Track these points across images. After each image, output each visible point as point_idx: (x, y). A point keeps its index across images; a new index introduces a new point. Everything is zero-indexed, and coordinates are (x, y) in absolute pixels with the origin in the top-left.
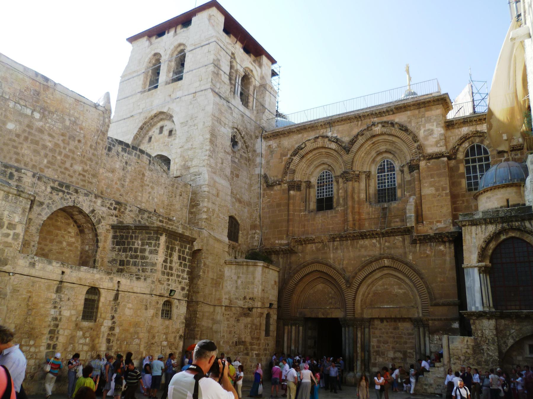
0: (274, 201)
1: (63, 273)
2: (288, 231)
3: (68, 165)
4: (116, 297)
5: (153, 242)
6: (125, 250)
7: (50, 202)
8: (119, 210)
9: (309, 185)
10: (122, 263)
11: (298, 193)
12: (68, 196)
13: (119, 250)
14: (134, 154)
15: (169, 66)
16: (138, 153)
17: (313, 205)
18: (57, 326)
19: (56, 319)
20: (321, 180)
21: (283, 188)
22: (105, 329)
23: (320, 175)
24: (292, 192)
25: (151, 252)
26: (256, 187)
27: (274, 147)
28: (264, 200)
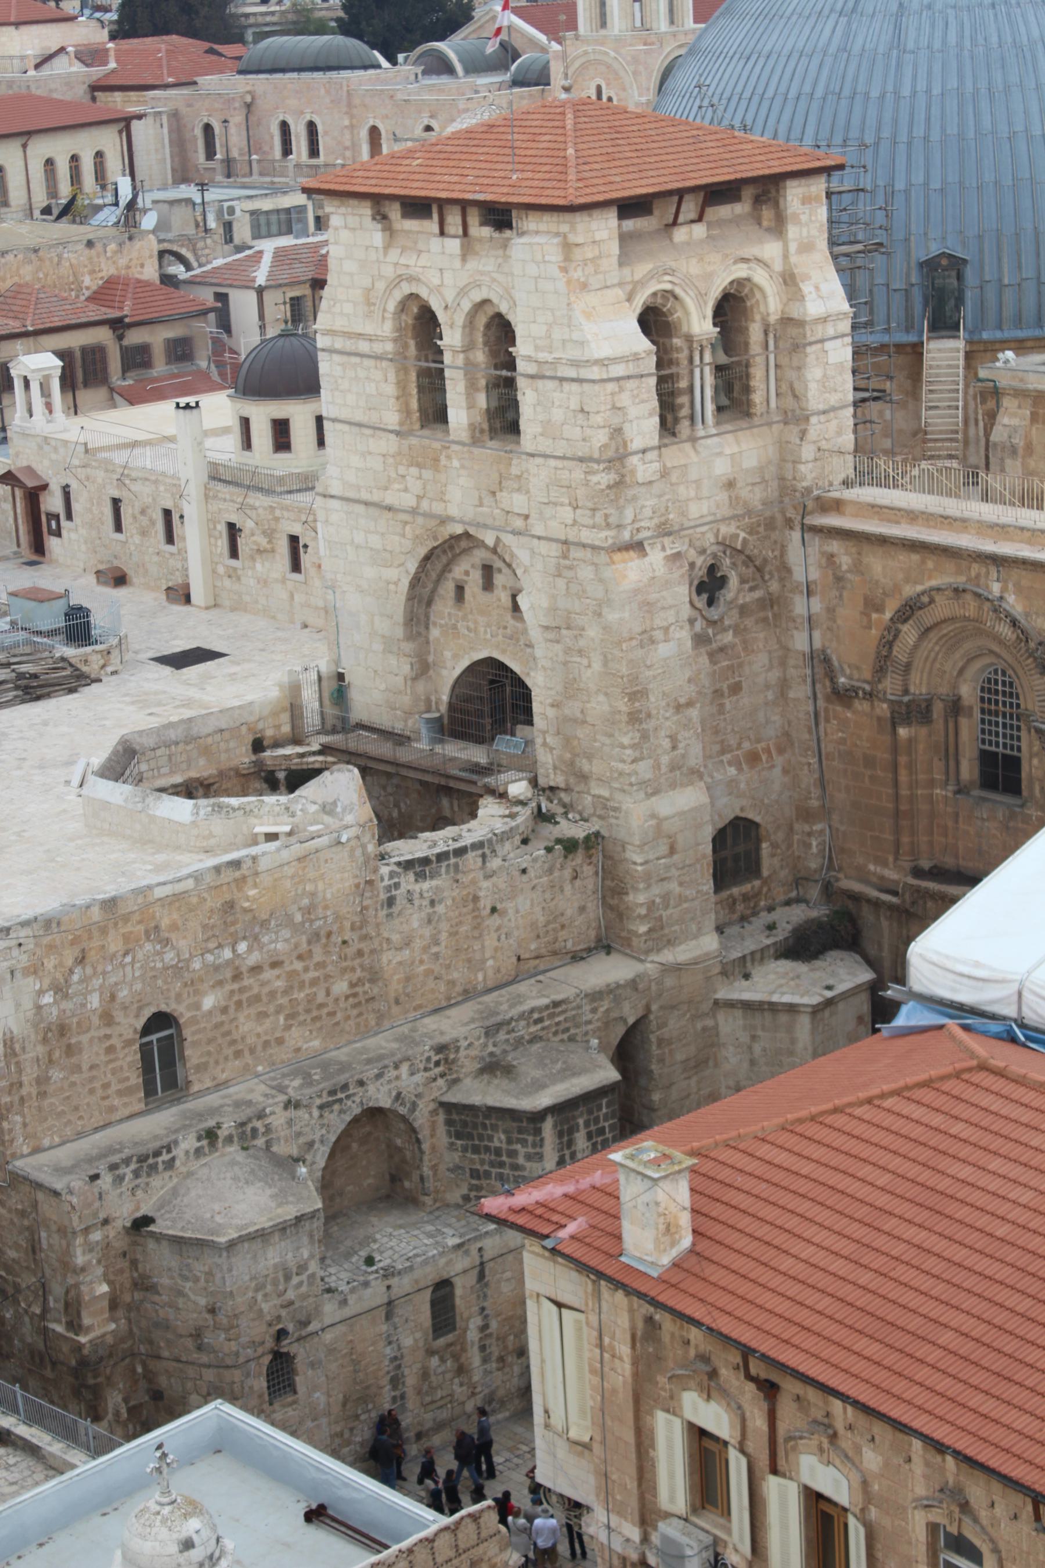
0: (856, 745)
1: (389, 1287)
2: (897, 844)
3: (321, 998)
4: (481, 1276)
5: (530, 1139)
6: (476, 1150)
7: (324, 1131)
8: (446, 1060)
9: (955, 708)
10: (475, 1174)
11: (923, 731)
12: (349, 1103)
14: (443, 870)
15: (469, 366)
16: (453, 861)
17: (968, 769)
18: (399, 1367)
19: (395, 1358)
20: (989, 691)
21: (878, 711)
22: (473, 1335)
23: (985, 675)
24: (903, 732)
25: (529, 1157)
26: (800, 692)
27: (845, 567)
28: (829, 730)
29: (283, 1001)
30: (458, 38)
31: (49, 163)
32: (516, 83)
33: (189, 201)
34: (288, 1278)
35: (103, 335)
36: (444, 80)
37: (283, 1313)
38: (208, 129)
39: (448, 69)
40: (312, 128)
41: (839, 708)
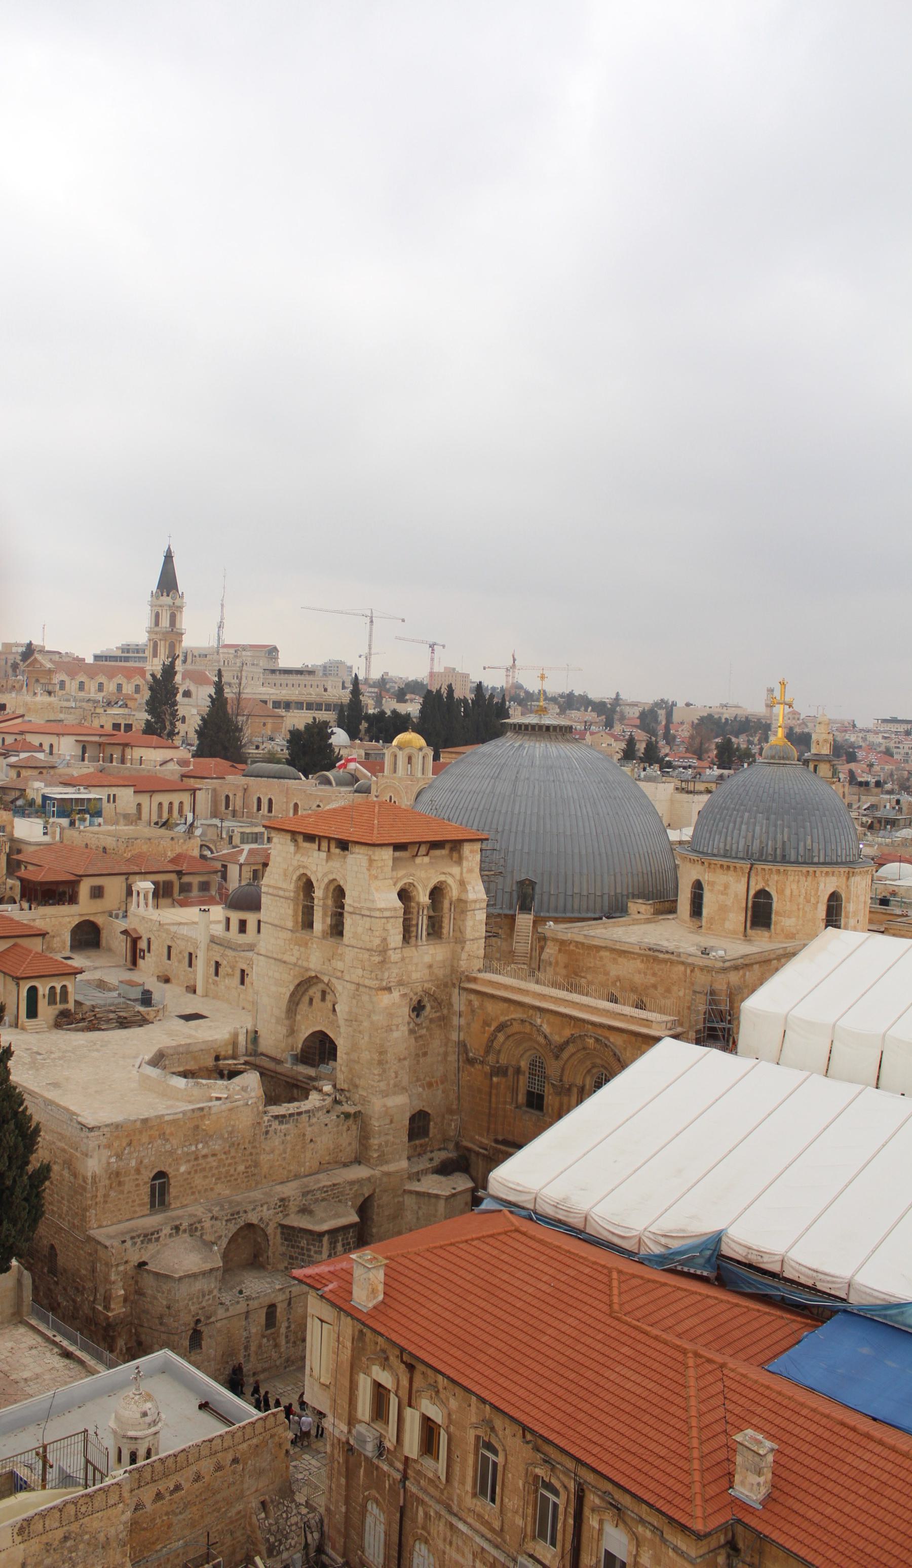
2: (489, 1129)
3: (232, 1172)
4: (289, 1304)
6: (293, 1247)
9: (518, 1071)
10: (291, 1257)
11: (504, 1080)
13: (288, 1246)
15: (325, 906)
16: (296, 1117)
17: (522, 1098)
19: (247, 1338)
22: (283, 1330)
24: (495, 1079)
25: (316, 1252)
26: (452, 1058)
29: (216, 1172)
30: (334, 771)
31: (160, 804)
32: (356, 791)
33: (216, 826)
34: (204, 1296)
35: (173, 877)
36: (327, 787)
37: (200, 1312)
38: (227, 797)
39: (328, 782)
40: (270, 801)
41: (468, 1067)
